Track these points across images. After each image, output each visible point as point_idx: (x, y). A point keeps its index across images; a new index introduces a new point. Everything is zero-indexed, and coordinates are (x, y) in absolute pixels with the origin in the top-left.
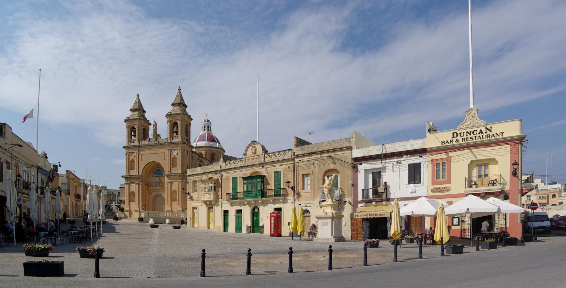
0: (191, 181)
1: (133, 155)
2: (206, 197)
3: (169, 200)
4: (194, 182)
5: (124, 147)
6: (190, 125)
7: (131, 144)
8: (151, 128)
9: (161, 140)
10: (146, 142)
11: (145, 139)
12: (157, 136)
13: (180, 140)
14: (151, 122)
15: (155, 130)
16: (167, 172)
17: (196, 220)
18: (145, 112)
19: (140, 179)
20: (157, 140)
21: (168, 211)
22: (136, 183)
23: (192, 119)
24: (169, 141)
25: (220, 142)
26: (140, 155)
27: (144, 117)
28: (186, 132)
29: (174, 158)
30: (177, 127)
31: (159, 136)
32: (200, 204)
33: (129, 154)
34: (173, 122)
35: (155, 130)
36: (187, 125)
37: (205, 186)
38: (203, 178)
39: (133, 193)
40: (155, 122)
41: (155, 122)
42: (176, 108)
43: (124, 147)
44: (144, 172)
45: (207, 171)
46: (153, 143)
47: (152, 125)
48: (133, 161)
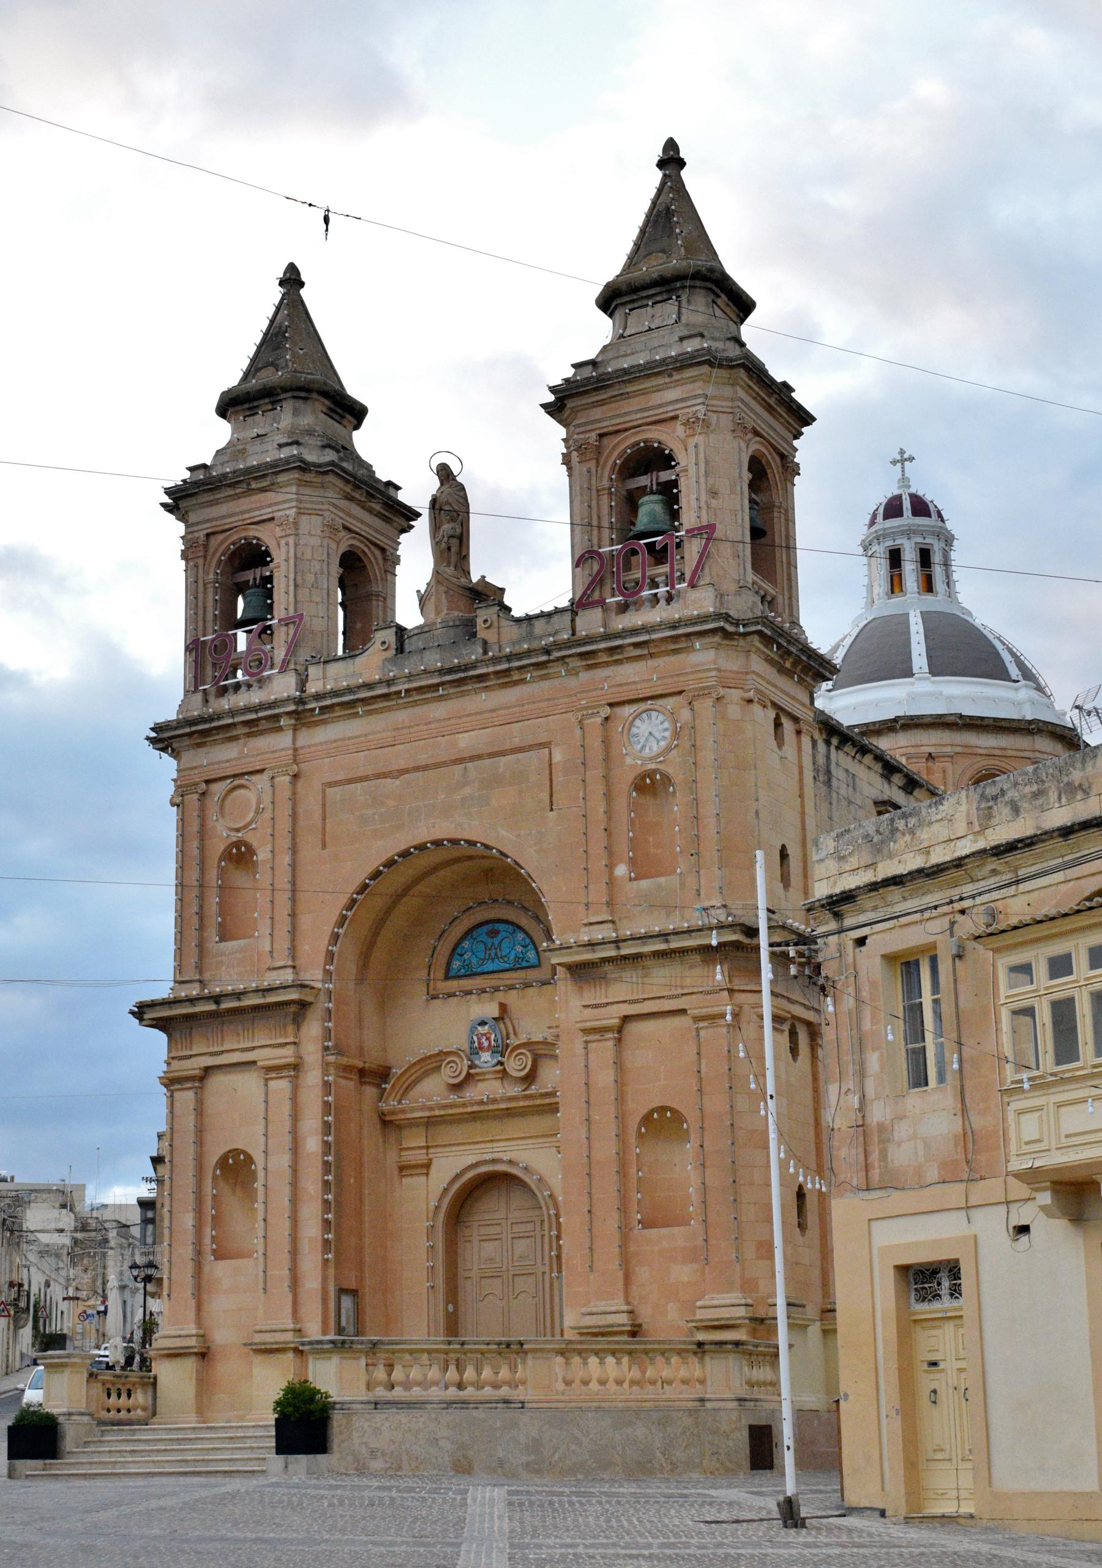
0: (870, 961)
1: (249, 796)
2: (1073, 1120)
3: (608, 1223)
4: (906, 966)
5: (164, 738)
6: (791, 470)
7: (225, 703)
8: (415, 561)
9: (511, 632)
10: (371, 665)
11: (357, 638)
12: (468, 598)
13: (700, 602)
14: (417, 490)
15: (453, 546)
16: (572, 928)
17: (943, 1426)
18: (356, 413)
19: (312, 1029)
20: (468, 629)
21: (597, 1340)
22: (273, 1070)
23: (806, 418)
24: (590, 622)
25: (1046, 677)
26: (310, 803)
27: (347, 451)
28: (757, 533)
29: (650, 784)
30: (669, 493)
31: (487, 595)
32: (991, 1226)
33: (191, 795)
34: (618, 448)
35: (453, 546)
36: (758, 469)
37: (1062, 987)
38: (1018, 906)
39: (236, 1168)
40: (445, 473)
41: (445, 473)
42: (640, 319)
43: (164, 738)
44: (348, 951)
45: (1059, 816)
46: (434, 660)
47: (422, 526)
48: (240, 855)
